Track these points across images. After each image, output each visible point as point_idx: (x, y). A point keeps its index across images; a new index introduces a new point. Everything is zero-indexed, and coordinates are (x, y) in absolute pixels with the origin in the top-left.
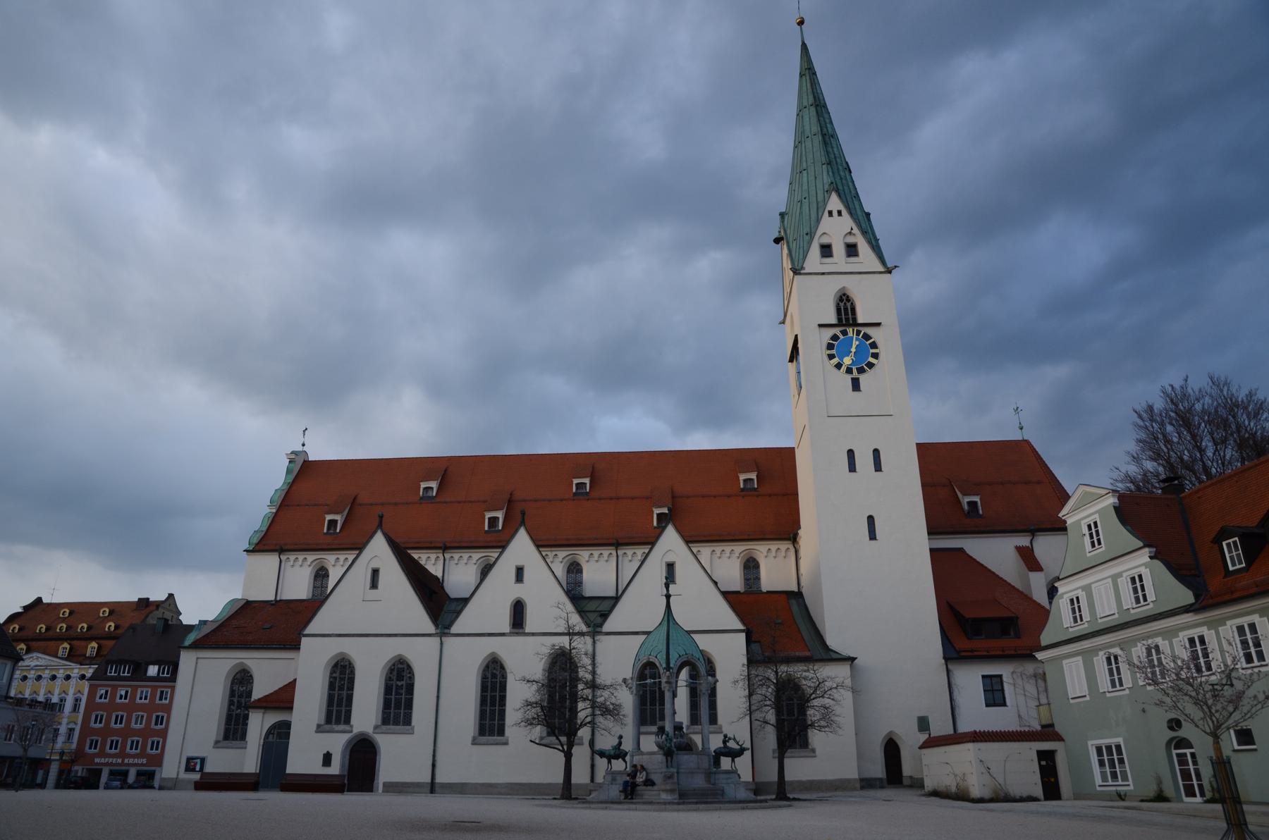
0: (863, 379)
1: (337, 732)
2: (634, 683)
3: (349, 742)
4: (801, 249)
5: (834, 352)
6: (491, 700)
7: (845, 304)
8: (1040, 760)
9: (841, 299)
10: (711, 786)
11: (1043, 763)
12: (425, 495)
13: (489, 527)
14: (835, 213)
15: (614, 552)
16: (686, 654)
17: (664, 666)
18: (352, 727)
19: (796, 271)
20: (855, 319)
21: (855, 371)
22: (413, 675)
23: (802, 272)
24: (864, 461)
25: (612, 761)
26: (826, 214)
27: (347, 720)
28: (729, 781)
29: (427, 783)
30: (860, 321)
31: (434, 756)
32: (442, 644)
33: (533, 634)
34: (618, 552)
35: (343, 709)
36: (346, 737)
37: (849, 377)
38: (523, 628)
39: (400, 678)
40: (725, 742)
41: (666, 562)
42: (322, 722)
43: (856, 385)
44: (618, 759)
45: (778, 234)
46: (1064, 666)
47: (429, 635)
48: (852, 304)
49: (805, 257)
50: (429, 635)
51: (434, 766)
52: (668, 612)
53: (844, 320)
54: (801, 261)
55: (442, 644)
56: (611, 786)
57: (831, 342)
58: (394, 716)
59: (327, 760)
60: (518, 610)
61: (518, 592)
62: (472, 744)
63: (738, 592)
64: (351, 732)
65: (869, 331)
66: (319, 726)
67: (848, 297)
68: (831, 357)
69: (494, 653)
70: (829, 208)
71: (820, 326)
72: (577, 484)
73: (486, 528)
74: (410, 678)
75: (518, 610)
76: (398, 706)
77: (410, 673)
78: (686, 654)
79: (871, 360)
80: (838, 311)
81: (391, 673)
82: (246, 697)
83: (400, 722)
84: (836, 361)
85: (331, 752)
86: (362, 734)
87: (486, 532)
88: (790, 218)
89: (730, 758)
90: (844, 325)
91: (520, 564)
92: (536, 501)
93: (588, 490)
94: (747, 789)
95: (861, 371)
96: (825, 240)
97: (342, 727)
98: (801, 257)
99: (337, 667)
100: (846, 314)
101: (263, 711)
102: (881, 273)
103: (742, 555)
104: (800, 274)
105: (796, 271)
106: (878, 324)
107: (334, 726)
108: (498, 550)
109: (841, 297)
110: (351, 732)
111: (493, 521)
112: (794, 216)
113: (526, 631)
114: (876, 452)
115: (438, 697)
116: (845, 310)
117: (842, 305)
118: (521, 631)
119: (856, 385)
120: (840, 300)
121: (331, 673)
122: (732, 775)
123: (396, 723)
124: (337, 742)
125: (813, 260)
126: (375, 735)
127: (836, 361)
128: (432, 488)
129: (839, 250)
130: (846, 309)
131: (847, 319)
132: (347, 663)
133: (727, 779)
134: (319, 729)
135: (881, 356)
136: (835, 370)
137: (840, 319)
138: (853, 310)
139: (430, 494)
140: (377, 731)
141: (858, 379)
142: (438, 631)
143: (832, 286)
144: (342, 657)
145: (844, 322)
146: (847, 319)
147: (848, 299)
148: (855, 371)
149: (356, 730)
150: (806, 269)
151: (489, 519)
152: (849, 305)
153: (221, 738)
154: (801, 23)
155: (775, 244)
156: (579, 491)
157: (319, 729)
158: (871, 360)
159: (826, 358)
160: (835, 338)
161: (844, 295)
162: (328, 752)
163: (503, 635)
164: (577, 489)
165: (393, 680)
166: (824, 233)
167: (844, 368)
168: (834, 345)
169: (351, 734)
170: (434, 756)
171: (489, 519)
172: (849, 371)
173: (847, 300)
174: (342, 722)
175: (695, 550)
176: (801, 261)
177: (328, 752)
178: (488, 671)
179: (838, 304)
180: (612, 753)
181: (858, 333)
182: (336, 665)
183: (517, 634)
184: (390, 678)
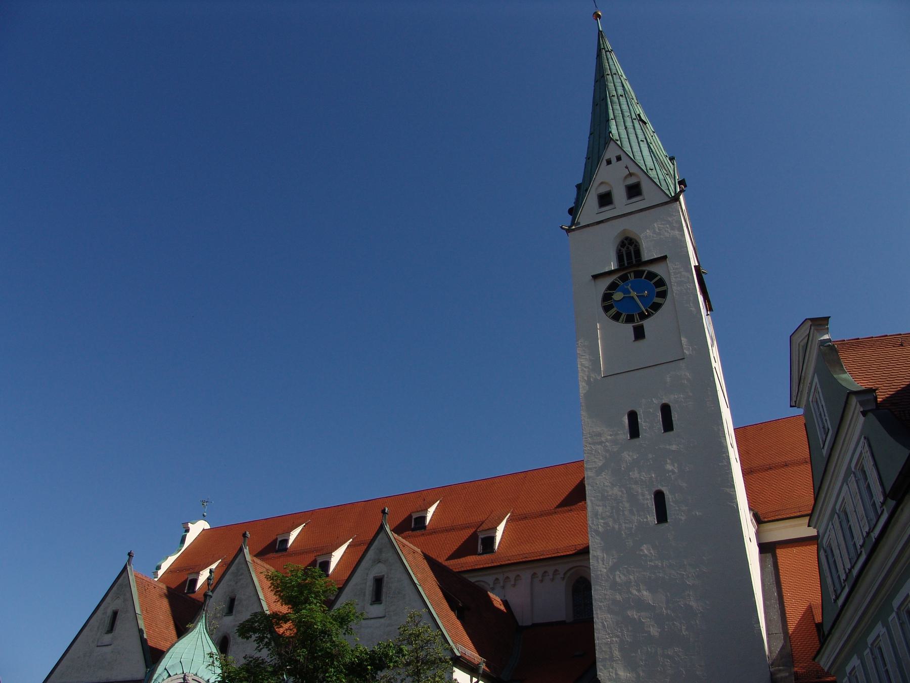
0: (647, 324)
9: (622, 244)
14: (614, 160)
21: (637, 317)
26: (604, 162)
37: (630, 327)
43: (639, 334)
48: (636, 246)
63: (562, 623)
65: (654, 269)
70: (607, 156)
71: (595, 277)
95: (643, 317)
96: (603, 190)
102: (666, 203)
103: (568, 574)
106: (664, 258)
114: (666, 410)
117: (624, 250)
119: (639, 334)
120: (621, 246)
129: (619, 195)
141: (642, 327)
152: (632, 248)
164: (415, 524)
166: (602, 183)
167: (623, 317)
179: (620, 250)
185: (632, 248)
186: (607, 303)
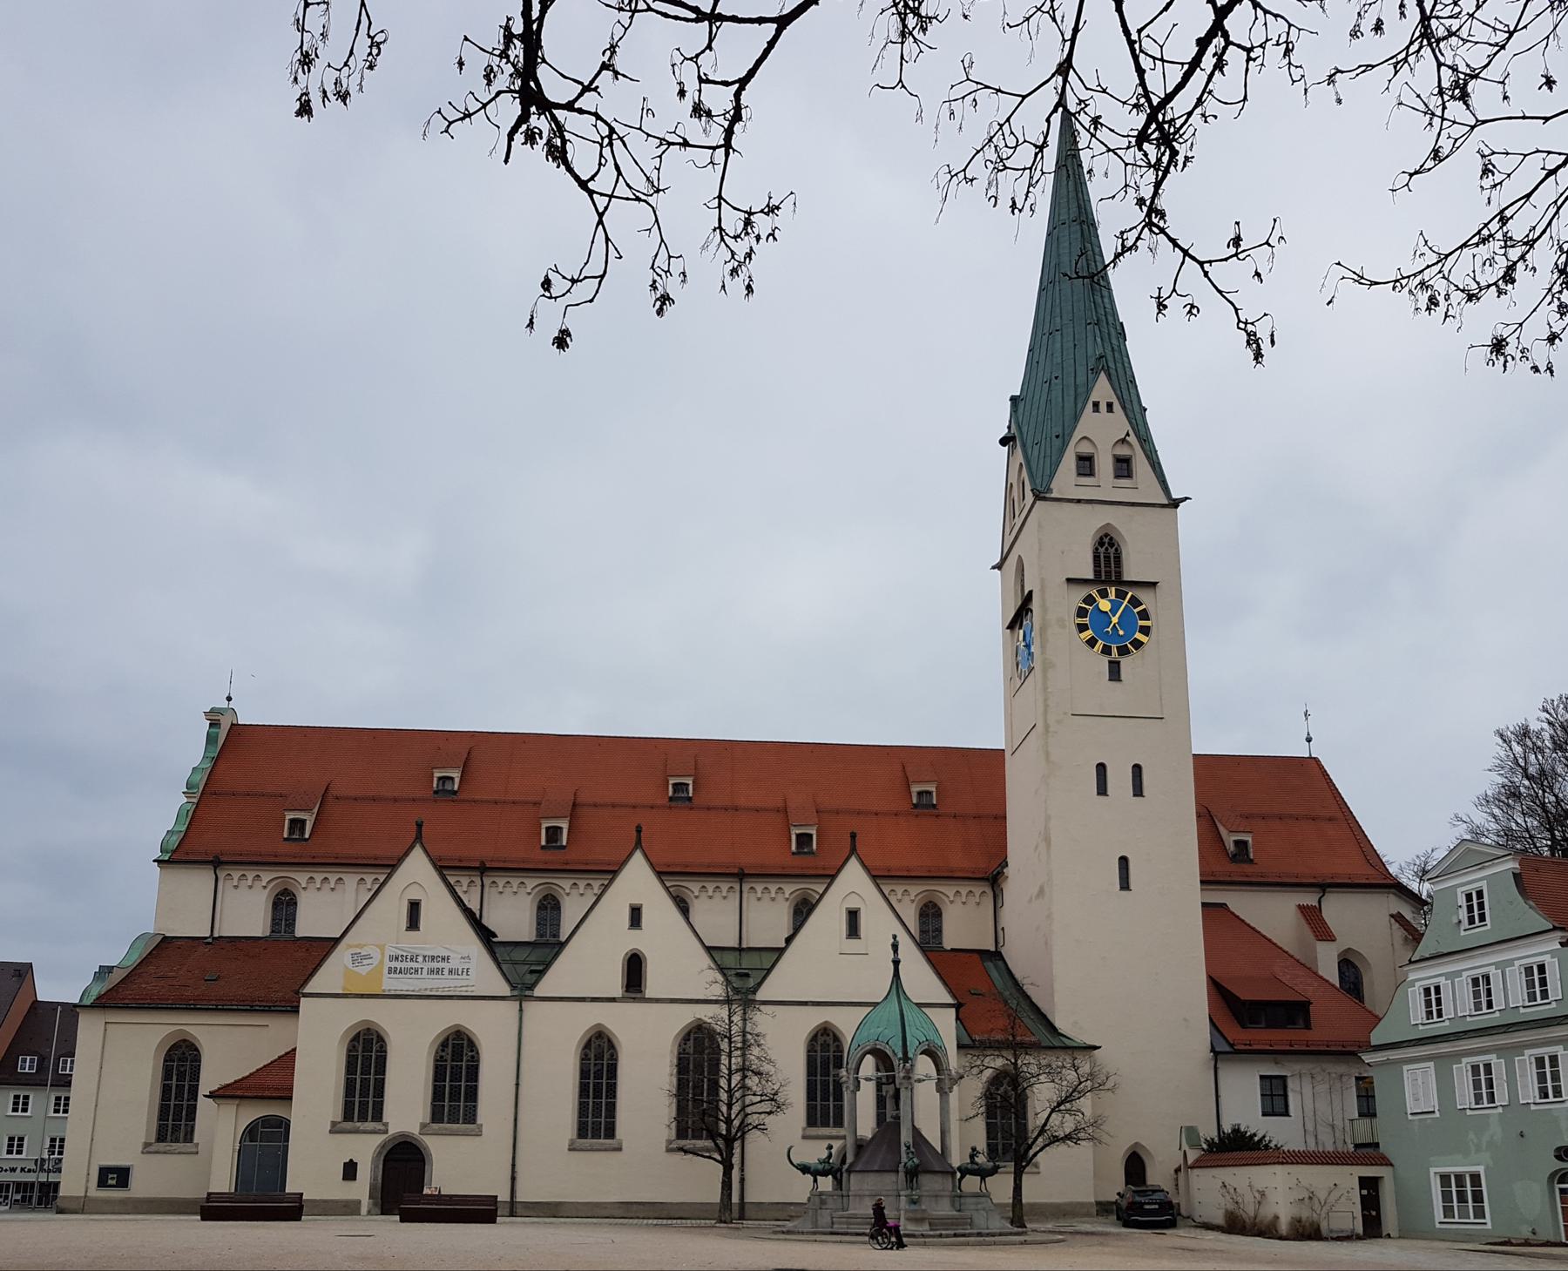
1: (365, 1132)
2: (851, 1077)
3: (383, 1146)
4: (1048, 460)
5: (1086, 620)
6: (594, 1090)
7: (1107, 549)
8: (1361, 1188)
9: (1101, 543)
10: (955, 1213)
11: (1365, 1192)
15: (737, 887)
16: (927, 1040)
17: (900, 1055)
18: (386, 1125)
19: (1039, 496)
20: (1119, 574)
21: (1115, 651)
22: (478, 1053)
23: (1047, 495)
24: (1120, 780)
25: (819, 1178)
27: (378, 1116)
28: (980, 1206)
30: (1126, 578)
32: (521, 1010)
33: (657, 1001)
34: (743, 885)
36: (380, 1139)
37: (1106, 659)
38: (641, 992)
39: (458, 1055)
40: (972, 1157)
41: (847, 908)
42: (339, 1119)
43: (1115, 673)
44: (826, 1176)
45: (1007, 431)
46: (1405, 1072)
47: (503, 998)
48: (1116, 550)
49: (1052, 476)
50: (503, 998)
52: (897, 982)
53: (1103, 574)
54: (1046, 479)
55: (521, 1010)
56: (819, 1211)
57: (1084, 605)
58: (450, 1111)
59: (350, 1171)
60: (635, 967)
66: (334, 1124)
67: (1111, 539)
68: (1082, 628)
69: (599, 1024)
71: (1069, 580)
73: (543, 843)
74: (473, 1057)
75: (635, 967)
77: (472, 1051)
78: (927, 1040)
79: (1139, 636)
80: (1096, 558)
81: (443, 1051)
82: (191, 1081)
84: (1088, 634)
86: (403, 1135)
87: (543, 847)
88: (1028, 407)
89: (979, 1178)
90: (1103, 582)
91: (636, 902)
92: (614, 806)
94: (1003, 1218)
95: (1123, 651)
97: (370, 1125)
98: (1047, 472)
100: (1108, 564)
104: (1045, 499)
105: (1039, 496)
106: (1154, 584)
107: (359, 1124)
108: (607, 877)
109: (1101, 538)
111: (554, 833)
112: (1035, 406)
113: (647, 997)
116: (1107, 552)
117: (1102, 550)
118: (638, 995)
119: (1115, 673)
120: (1099, 543)
121: (349, 1051)
122: (983, 1199)
124: (365, 1148)
125: (1066, 479)
127: (1088, 634)
130: (1107, 558)
131: (1108, 573)
132: (375, 1037)
133: (978, 1204)
134: (335, 1129)
135: (1153, 631)
136: (1087, 648)
137: (1097, 572)
138: (1118, 558)
140: (424, 1131)
141: (1119, 663)
142: (516, 993)
143: (1091, 523)
144: (366, 1027)
145: (1103, 578)
146: (1108, 573)
147: (1111, 544)
148: (1115, 651)
150: (1054, 491)
151: (548, 829)
152: (1112, 551)
153: (153, 1139)
155: (1000, 446)
157: (335, 1129)
158: (1139, 636)
159: (1074, 629)
160: (1089, 600)
161: (1106, 535)
162: (351, 1160)
163: (613, 1000)
165: (446, 1061)
168: (1087, 610)
169: (386, 1136)
171: (548, 829)
172: (1106, 650)
173: (1109, 544)
174: (370, 1118)
175: (886, 891)
176: (1046, 479)
177: (351, 1160)
178: (590, 1049)
179: (1097, 549)
180: (820, 1167)
181: (1121, 595)
182: (356, 1038)
183: (634, 1000)
185: (1112, 551)
186: (1079, 620)
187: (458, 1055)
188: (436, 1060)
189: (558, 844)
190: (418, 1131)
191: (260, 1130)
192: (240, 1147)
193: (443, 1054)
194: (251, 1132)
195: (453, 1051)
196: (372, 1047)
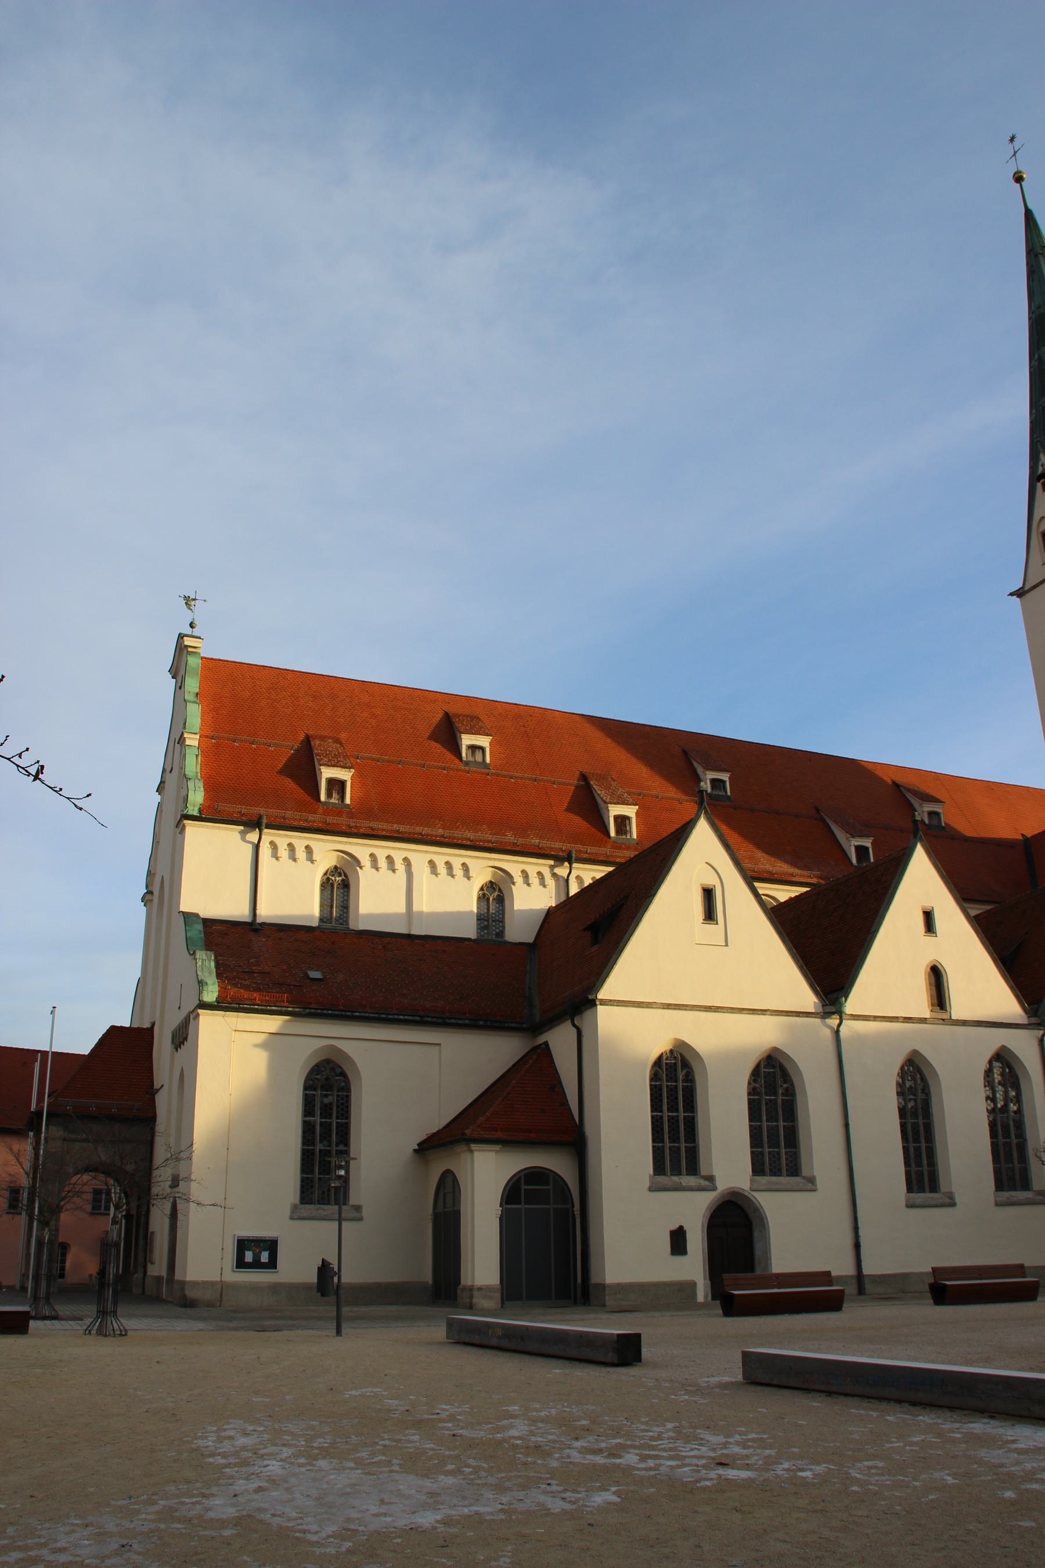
12: (471, 759)
13: (618, 832)
18: (711, 1179)
22: (792, 1085)
27: (693, 1168)
29: (851, 1277)
31: (856, 1229)
33: (964, 1023)
35: (667, 1144)
39: (771, 1089)
51: (857, 1246)
59: (678, 1241)
61: (931, 950)
62: (908, 1206)
64: (714, 1189)
72: (715, 782)
74: (787, 1089)
76: (774, 1143)
77: (785, 1082)
81: (755, 1081)
83: (780, 1170)
85: (685, 1229)
93: (729, 794)
99: (660, 1067)
101: (497, 1147)
110: (714, 1189)
115: (847, 1125)
118: (945, 1016)
123: (776, 1172)
126: (755, 1194)
128: (482, 749)
139: (479, 757)
149: (723, 1184)
151: (617, 818)
154: (1019, 179)
156: (714, 793)
162: (681, 1228)
163: (923, 1021)
164: (713, 788)
170: (856, 1229)
177: (681, 1228)
184: (754, 1089)
187: (771, 1089)
188: (749, 1094)
189: (628, 837)
190: (748, 1185)
191: (524, 1187)
192: (502, 1211)
193: (785, 1086)
194: (512, 1194)
195: (765, 1082)
196: (676, 1075)
